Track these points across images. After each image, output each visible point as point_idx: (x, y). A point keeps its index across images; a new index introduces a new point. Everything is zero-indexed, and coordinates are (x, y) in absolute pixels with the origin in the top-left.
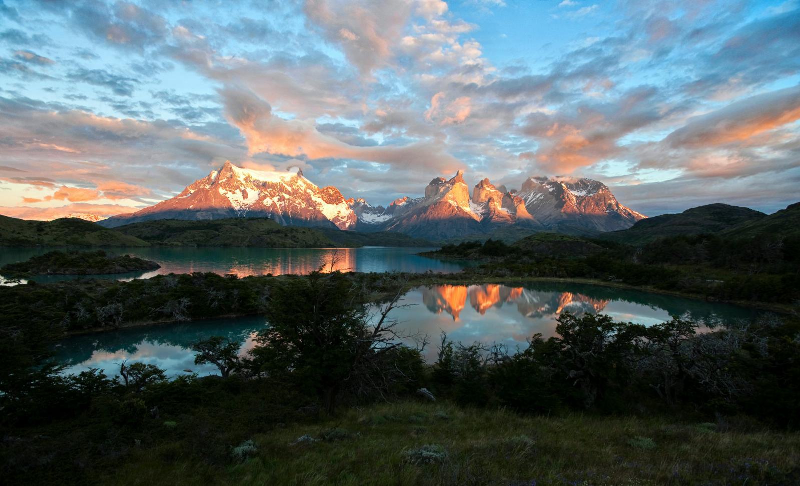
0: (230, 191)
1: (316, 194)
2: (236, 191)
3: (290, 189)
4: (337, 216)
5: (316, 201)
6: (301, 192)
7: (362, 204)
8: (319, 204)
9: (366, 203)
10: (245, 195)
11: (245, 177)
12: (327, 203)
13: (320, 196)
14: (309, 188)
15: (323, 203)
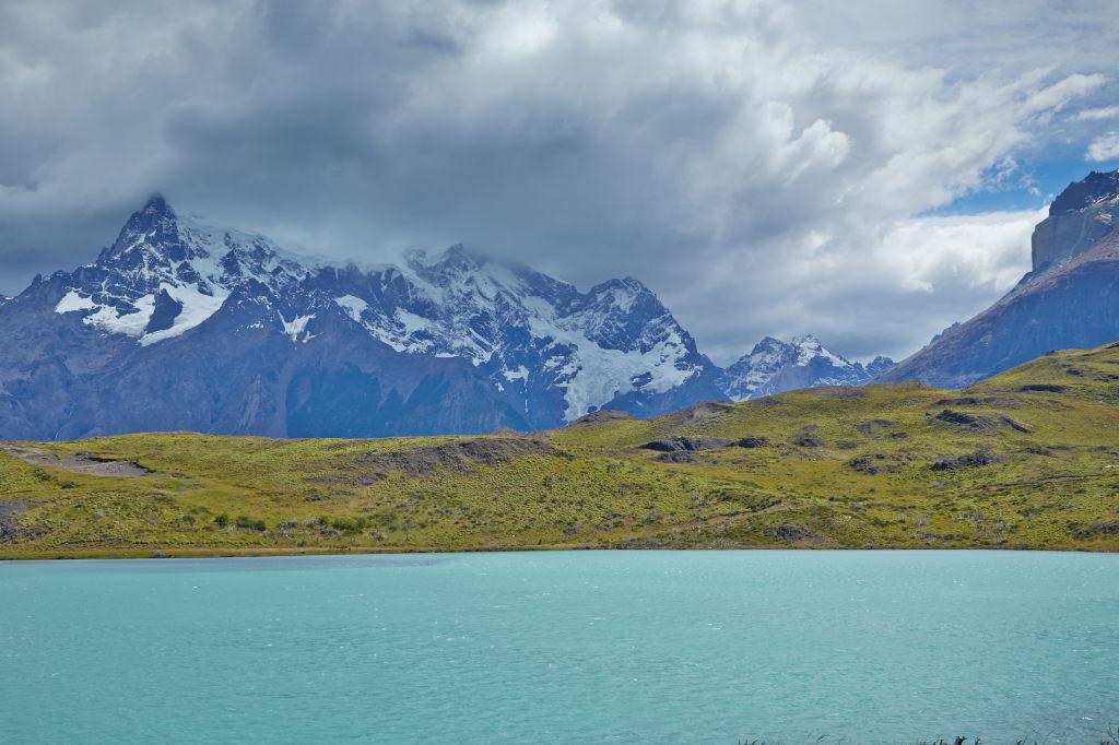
0: (112, 303)
1: (563, 315)
2: (139, 304)
3: (435, 294)
4: (637, 395)
5: (549, 340)
6: (481, 303)
7: (811, 355)
8: (565, 351)
9: (825, 353)
10: (167, 310)
11: (227, 250)
12: (604, 345)
13: (581, 321)
14: (535, 293)
15: (588, 352)
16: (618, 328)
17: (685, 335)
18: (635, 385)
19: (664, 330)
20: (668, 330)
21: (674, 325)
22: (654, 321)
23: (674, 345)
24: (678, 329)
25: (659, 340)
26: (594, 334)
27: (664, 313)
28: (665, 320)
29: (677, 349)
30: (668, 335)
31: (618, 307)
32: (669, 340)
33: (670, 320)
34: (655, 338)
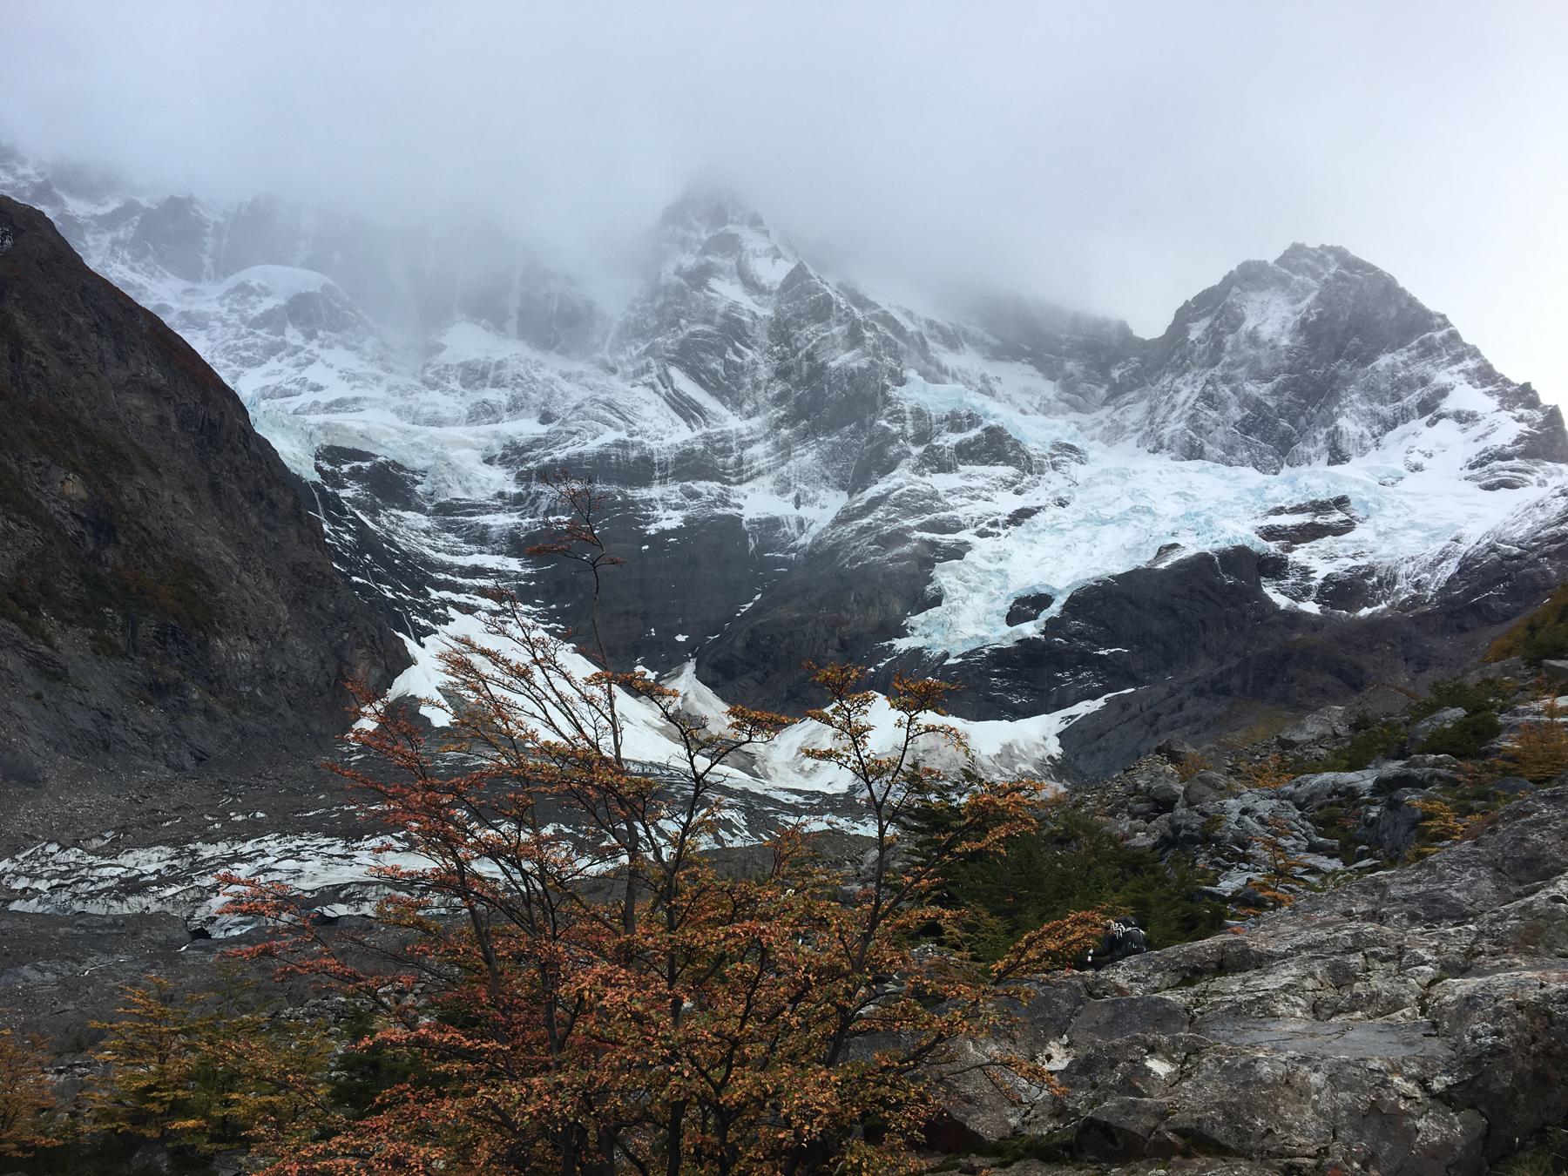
16: (1245, 401)
17: (1523, 396)
18: (1270, 533)
19: (1424, 382)
20: (1441, 377)
21: (1470, 364)
22: (1384, 361)
23: (1464, 418)
24: (1486, 376)
25: (1404, 416)
26: (1167, 432)
27: (1430, 328)
28: (1428, 350)
29: (1476, 430)
30: (1443, 393)
31: (1253, 339)
32: (1448, 405)
33: (1454, 348)
34: (1386, 411)
